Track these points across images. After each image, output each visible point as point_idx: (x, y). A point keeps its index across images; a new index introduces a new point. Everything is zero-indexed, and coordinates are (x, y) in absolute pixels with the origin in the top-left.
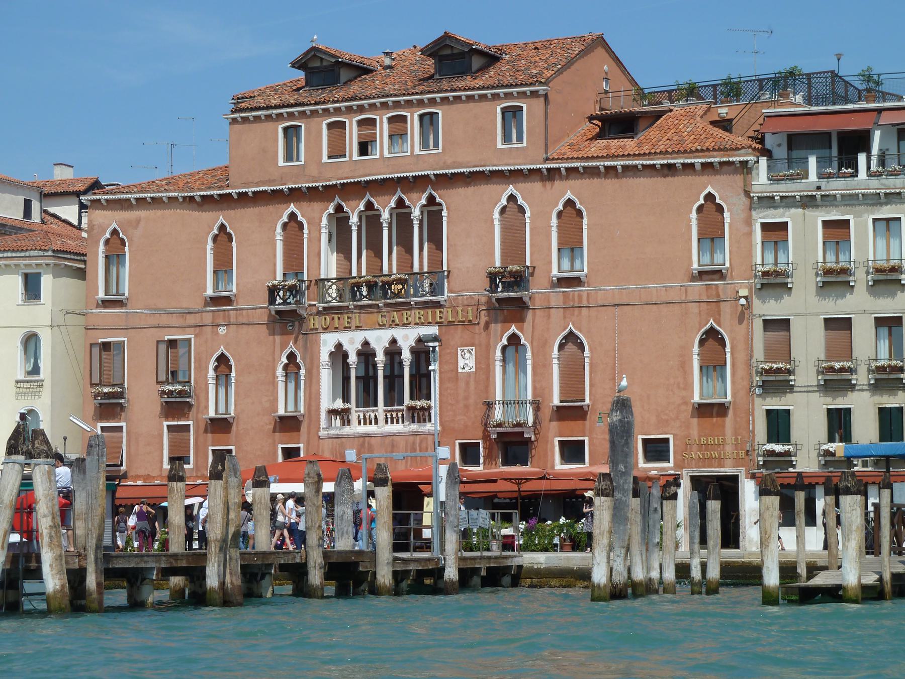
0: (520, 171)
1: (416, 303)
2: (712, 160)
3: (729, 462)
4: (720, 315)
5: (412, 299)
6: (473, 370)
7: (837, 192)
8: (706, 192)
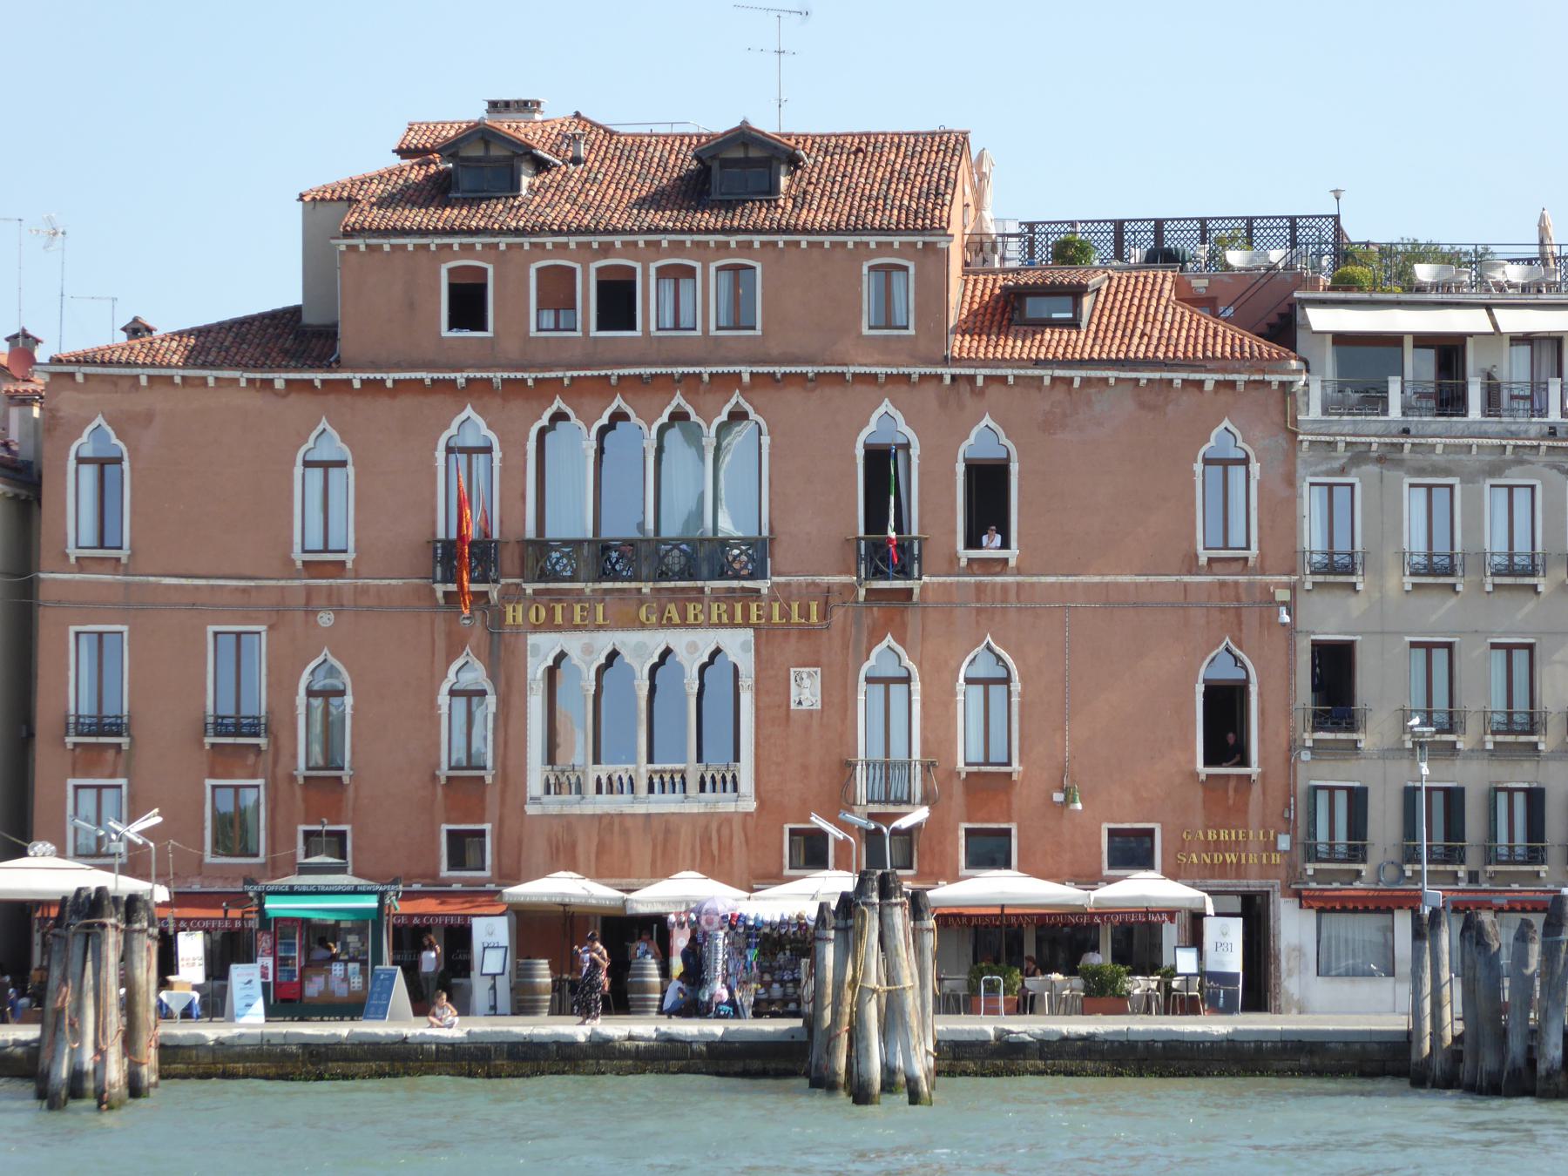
5: (708, 583)
6: (818, 706)
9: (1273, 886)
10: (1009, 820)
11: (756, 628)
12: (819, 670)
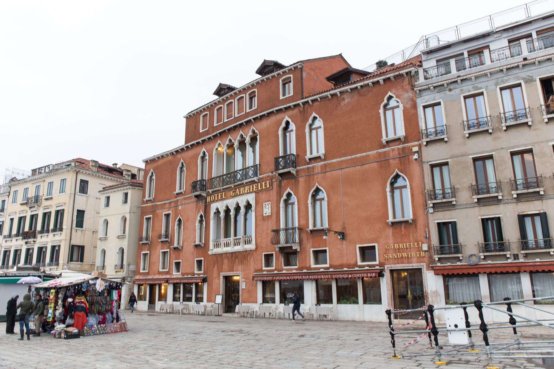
1: (246, 183)
3: (414, 260)
7: (472, 75)
8: (388, 95)
9: (423, 266)
10: (326, 247)
11: (255, 192)
12: (270, 202)
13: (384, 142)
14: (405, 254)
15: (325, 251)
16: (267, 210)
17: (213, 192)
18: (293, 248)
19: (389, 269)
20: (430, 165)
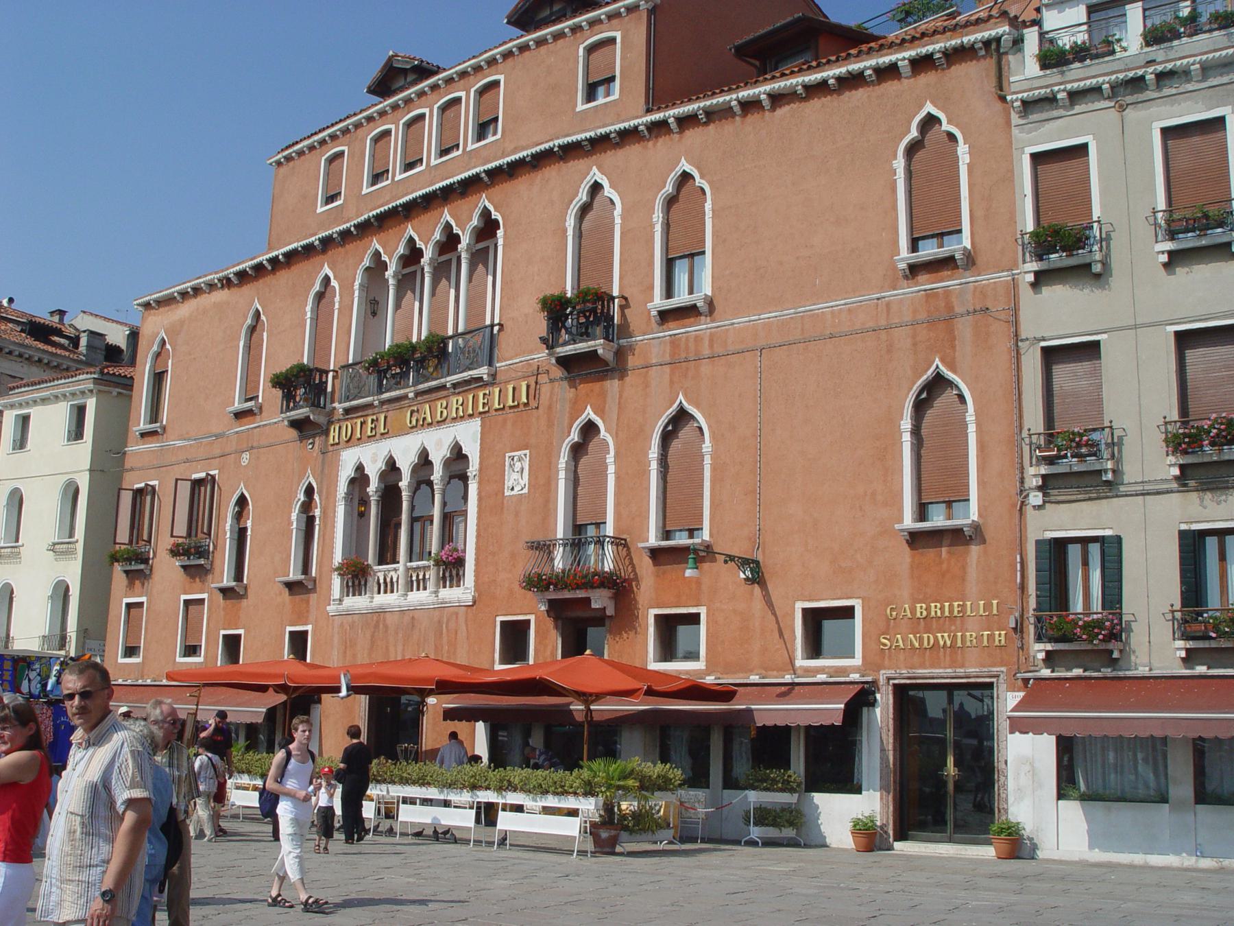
0: (605, 138)
1: (455, 386)
2: (930, 48)
4: (953, 347)
5: (449, 379)
6: (525, 491)
9: (998, 676)
12: (527, 452)
13: (903, 265)
14: (946, 635)
15: (694, 619)
16: (515, 476)
17: (347, 411)
18: (594, 605)
19: (892, 682)
20: (1043, 348)
